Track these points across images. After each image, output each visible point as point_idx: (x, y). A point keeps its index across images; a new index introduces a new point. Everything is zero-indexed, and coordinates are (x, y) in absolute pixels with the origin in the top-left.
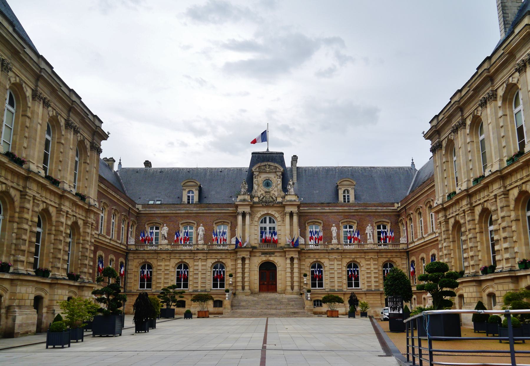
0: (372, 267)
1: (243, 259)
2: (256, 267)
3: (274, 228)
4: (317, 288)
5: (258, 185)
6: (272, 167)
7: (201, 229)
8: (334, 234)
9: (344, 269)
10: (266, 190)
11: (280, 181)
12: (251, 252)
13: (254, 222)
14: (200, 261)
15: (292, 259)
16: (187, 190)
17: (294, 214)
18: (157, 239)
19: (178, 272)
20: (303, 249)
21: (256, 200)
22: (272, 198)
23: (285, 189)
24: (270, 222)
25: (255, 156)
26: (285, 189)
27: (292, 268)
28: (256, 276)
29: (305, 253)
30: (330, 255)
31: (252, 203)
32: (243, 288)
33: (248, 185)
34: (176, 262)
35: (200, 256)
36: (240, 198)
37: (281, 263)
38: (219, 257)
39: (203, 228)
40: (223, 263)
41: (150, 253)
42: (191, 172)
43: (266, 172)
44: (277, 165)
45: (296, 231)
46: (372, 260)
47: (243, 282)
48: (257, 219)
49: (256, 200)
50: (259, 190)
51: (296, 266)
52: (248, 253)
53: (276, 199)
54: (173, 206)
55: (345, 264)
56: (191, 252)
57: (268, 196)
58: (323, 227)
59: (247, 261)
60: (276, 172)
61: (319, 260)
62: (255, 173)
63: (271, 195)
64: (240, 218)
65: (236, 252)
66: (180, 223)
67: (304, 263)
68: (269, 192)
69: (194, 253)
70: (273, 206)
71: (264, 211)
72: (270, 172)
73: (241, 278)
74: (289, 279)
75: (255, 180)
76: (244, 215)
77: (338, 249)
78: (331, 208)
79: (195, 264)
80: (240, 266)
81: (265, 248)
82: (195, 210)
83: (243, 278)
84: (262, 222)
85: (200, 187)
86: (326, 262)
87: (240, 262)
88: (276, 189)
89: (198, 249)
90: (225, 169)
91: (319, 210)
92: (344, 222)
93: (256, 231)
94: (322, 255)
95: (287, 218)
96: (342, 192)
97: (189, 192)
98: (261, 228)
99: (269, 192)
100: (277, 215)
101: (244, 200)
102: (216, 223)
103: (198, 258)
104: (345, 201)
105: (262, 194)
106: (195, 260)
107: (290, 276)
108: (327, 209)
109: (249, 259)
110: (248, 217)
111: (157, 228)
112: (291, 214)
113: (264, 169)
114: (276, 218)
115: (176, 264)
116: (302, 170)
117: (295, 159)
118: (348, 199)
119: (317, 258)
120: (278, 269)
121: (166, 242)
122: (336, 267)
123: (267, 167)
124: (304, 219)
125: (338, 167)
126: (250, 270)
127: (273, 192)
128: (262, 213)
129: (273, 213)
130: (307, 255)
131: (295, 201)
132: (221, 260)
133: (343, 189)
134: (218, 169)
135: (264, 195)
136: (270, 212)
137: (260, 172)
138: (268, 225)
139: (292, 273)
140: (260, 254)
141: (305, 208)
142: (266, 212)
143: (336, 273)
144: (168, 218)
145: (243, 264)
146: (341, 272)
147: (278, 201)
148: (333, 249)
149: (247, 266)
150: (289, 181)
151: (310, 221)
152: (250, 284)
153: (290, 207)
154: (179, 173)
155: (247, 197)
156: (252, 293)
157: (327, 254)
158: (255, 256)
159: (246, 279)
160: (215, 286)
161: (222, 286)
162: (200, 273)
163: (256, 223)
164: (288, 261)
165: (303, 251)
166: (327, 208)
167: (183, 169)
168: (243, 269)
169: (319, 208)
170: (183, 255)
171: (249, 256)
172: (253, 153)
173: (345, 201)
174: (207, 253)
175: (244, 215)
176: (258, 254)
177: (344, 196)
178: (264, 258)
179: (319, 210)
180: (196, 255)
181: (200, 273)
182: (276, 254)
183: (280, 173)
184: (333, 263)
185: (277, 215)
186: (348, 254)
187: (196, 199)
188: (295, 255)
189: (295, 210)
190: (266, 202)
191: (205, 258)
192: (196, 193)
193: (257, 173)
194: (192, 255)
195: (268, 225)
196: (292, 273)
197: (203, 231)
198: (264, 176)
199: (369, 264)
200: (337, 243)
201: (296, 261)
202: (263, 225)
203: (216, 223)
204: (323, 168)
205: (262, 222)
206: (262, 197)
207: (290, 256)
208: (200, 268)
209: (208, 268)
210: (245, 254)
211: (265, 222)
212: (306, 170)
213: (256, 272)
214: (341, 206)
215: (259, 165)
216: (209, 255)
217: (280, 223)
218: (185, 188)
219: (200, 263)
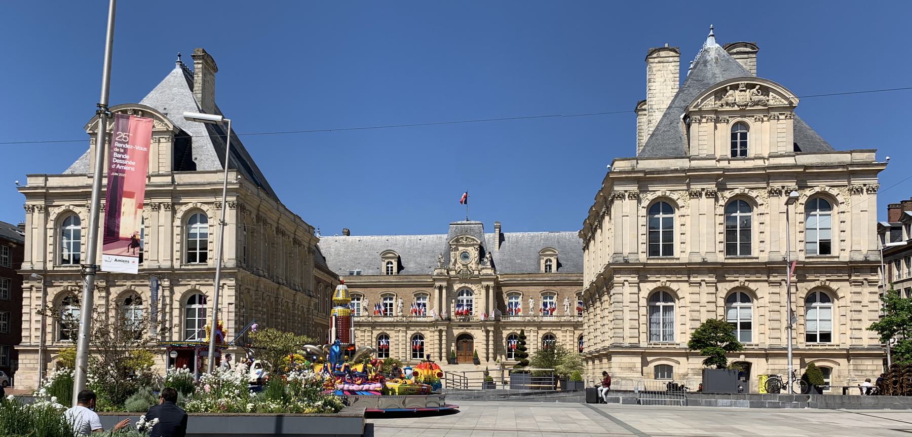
0: (568, 338)
3: (471, 301)
7: (400, 301)
10: (463, 262)
18: (358, 310)
49: (452, 273)
64: (437, 291)
77: (534, 321)
85: (399, 258)
88: (473, 262)
97: (388, 263)
110: (444, 291)
111: (358, 299)
121: (367, 313)
133: (545, 258)
145: (441, 336)
160: (415, 356)
161: (421, 356)
187: (395, 270)
192: (395, 265)
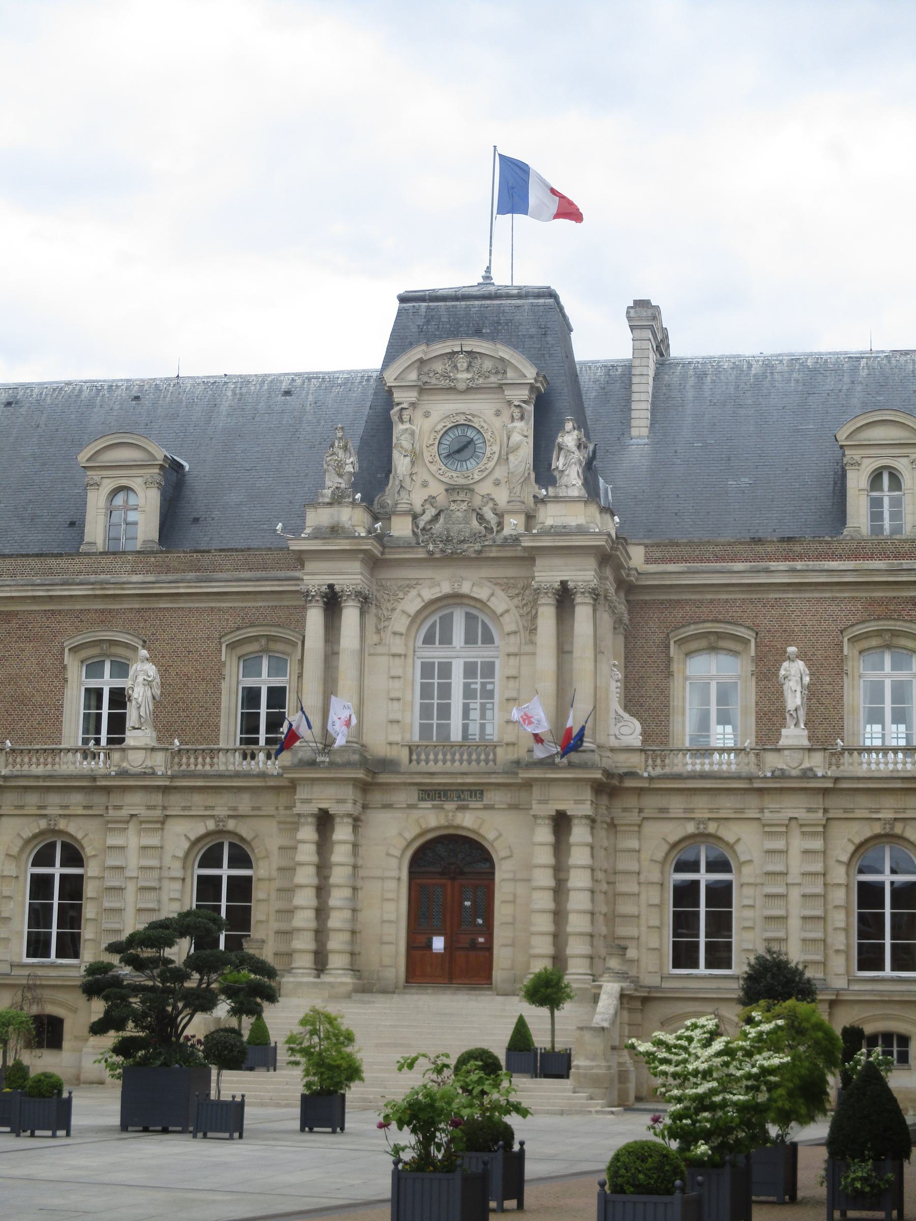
1: (324, 821)
2: (394, 862)
3: (489, 669)
4: (702, 970)
5: (415, 457)
6: (488, 365)
8: (794, 699)
9: (839, 874)
11: (522, 433)
12: (365, 787)
13: (388, 637)
14: (132, 826)
15: (561, 823)
16: (108, 486)
17: (579, 599)
19: (35, 878)
20: (632, 775)
21: (401, 528)
22: (481, 518)
23: (543, 471)
24: (470, 639)
25: (416, 312)
26: (543, 471)
27: (560, 870)
28: (390, 907)
29: (640, 791)
30: (769, 802)
31: (370, 545)
32: (320, 963)
33: (360, 454)
34: (27, 834)
35: (134, 804)
36: (317, 518)
37: (515, 842)
38: (221, 812)
39: (151, 670)
40: (242, 839)
41: (49, 789)
42: (146, 402)
43: (452, 390)
44: (504, 352)
45: (599, 678)
46: (795, 832)
47: (321, 933)
48: (400, 623)
50: (419, 480)
51: (579, 856)
52: (349, 792)
53: (500, 524)
54: (34, 562)
55: (842, 850)
56: (93, 786)
57: (459, 510)
58: (759, 659)
59: (342, 833)
60: (500, 387)
61: (712, 828)
62: (397, 396)
63: (477, 501)
64: (315, 618)
65: (293, 786)
66: (68, 644)
67: (633, 844)
68: (468, 489)
69: (107, 790)
70: (480, 559)
71: (442, 582)
72: (469, 390)
73: (311, 914)
74: (544, 923)
75: (399, 428)
76: (332, 602)
77: (808, 774)
78: (799, 565)
79: (111, 841)
80: (307, 853)
81: (432, 767)
82: (137, 581)
83: (321, 912)
84: (429, 639)
85: (172, 469)
86: (747, 842)
87: (308, 833)
89: (123, 774)
90: (309, 377)
91: (740, 570)
92: (867, 635)
93: (397, 684)
94: (727, 804)
95: (547, 616)
96: (864, 483)
98: (427, 669)
99: (468, 489)
100: (500, 602)
101: (335, 531)
102: (232, 646)
103: (125, 812)
104: (877, 529)
105: (431, 500)
106: (110, 825)
107: (551, 905)
108: (780, 571)
109: (356, 822)
110: (350, 615)
112: (564, 598)
113: (446, 376)
114: (497, 617)
115: (195, 843)
116: (684, 377)
117: (644, 317)
118: (896, 515)
119: (700, 821)
120: (502, 873)
122: (796, 865)
123: (462, 362)
124: (650, 622)
125: (871, 357)
126: (354, 875)
127: (485, 488)
128: (429, 594)
129: (482, 593)
130: (651, 803)
131: (581, 531)
132: (231, 825)
133: (869, 466)
134: (276, 379)
135: (442, 499)
136: (466, 588)
137: (423, 389)
138: (458, 654)
139: (560, 890)
140: (414, 799)
141: (671, 567)
142: (446, 588)
143: (795, 894)
144: (14, 624)
145: (324, 844)
146: (781, 890)
147: (507, 531)
148: (782, 775)
149: (340, 854)
150: (560, 427)
151: (692, 630)
152: (353, 942)
153: (557, 561)
154: (90, 404)
155: (353, 517)
156: (366, 985)
157: (753, 801)
158: (387, 806)
159: (337, 920)
162: (131, 888)
163: (398, 645)
164: (544, 834)
165: (629, 783)
166: (783, 566)
167: (112, 387)
168: (323, 868)
169: (739, 566)
170: (54, 799)
171: (356, 810)
172: (403, 299)
173: (877, 529)
174: (165, 790)
175: (332, 602)
176: (401, 798)
177: (876, 503)
178: (432, 819)
179: (740, 570)
180: (115, 799)
181: (131, 888)
182: (492, 797)
183: (524, 394)
184: (779, 844)
185: (500, 602)
186: (864, 801)
188: (579, 804)
189: (582, 574)
190: (448, 540)
191: (158, 813)
193: (412, 396)
194: (99, 799)
195: (458, 654)
196: (560, 890)
197: (149, 683)
198: (441, 411)
199: (785, 852)
200: (806, 743)
201: (579, 833)
202: (436, 654)
203: (232, 646)
204: (794, 360)
205: (429, 639)
206: (431, 512)
207: (551, 808)
208: (133, 861)
209: (167, 861)
210: (337, 798)
211: (446, 639)
212: (703, 371)
213: (393, 884)
214: (854, 555)
215: (418, 352)
216: (176, 802)
217: (512, 645)
218: (94, 475)
219: (132, 839)
